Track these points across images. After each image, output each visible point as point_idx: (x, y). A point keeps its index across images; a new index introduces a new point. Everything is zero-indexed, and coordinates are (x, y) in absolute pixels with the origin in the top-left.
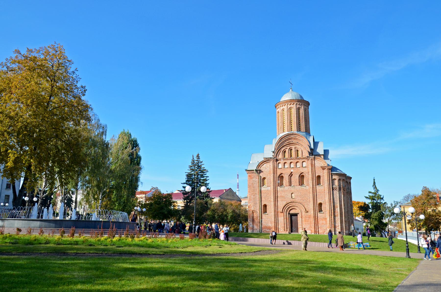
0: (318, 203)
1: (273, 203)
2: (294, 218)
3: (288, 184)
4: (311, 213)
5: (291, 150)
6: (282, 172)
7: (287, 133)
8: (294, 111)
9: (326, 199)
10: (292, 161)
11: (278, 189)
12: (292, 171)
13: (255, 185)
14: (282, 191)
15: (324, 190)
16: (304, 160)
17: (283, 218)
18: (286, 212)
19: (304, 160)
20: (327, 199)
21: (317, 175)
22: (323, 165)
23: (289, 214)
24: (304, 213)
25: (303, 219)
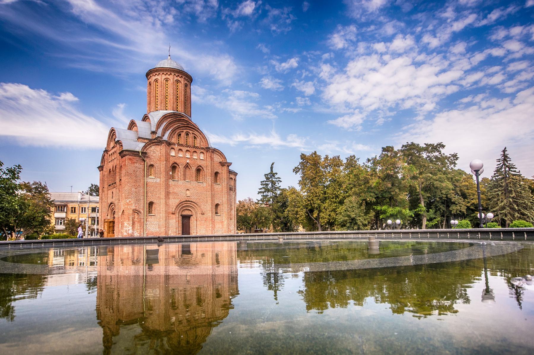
1: (163, 201)
2: (185, 221)
3: (182, 177)
4: (209, 214)
5: (187, 134)
6: (176, 161)
7: (172, 111)
8: (181, 86)
9: (224, 199)
10: (188, 149)
11: (170, 183)
12: (188, 161)
13: (138, 173)
14: (175, 185)
15: (222, 190)
17: (174, 221)
18: (179, 213)
19: (202, 151)
20: (225, 199)
21: (215, 171)
23: (181, 215)
24: (199, 215)
25: (198, 222)
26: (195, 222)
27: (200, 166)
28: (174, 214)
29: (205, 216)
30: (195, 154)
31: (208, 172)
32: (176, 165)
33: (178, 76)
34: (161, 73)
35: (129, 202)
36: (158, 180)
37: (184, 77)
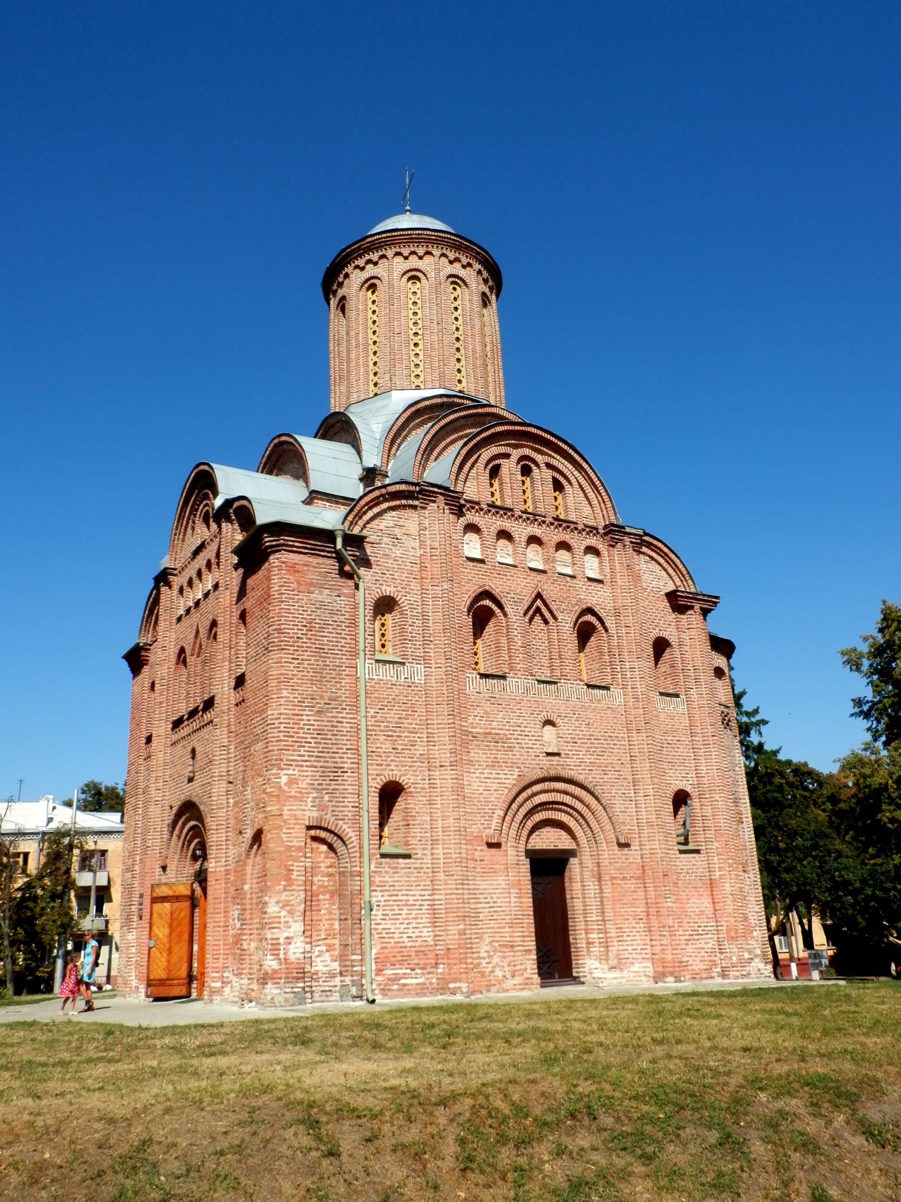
0: (670, 794)
10: (536, 530)
13: (328, 637)
16: (593, 541)
17: (501, 881)
19: (593, 541)
21: (655, 633)
22: (671, 587)
24: (609, 851)
25: (607, 890)
26: (592, 886)
27: (590, 611)
28: (497, 845)
29: (633, 854)
30: (563, 555)
31: (627, 637)
32: (487, 603)
33: (457, 260)
35: (291, 782)
36: (418, 673)
37: (477, 266)
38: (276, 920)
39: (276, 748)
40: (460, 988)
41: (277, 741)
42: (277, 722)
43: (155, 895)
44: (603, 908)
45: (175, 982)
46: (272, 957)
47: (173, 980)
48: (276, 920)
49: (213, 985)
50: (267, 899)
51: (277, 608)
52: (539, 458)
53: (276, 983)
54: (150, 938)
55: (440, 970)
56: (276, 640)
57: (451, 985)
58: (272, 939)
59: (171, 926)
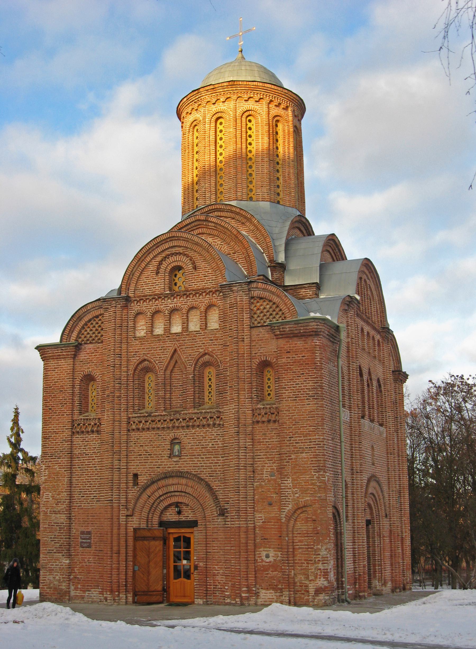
34: (267, 99)
38: (326, 559)
39: (322, 459)
40: (364, 595)
41: (322, 455)
42: (322, 443)
43: (137, 535)
44: (381, 553)
45: (154, 593)
46: (324, 579)
47: (153, 591)
48: (326, 559)
49: (243, 595)
50: (319, 547)
51: (319, 372)
52: (368, 281)
53: (327, 593)
54: (134, 565)
55: (357, 586)
56: (320, 392)
57: (361, 594)
58: (324, 569)
59: (149, 557)
